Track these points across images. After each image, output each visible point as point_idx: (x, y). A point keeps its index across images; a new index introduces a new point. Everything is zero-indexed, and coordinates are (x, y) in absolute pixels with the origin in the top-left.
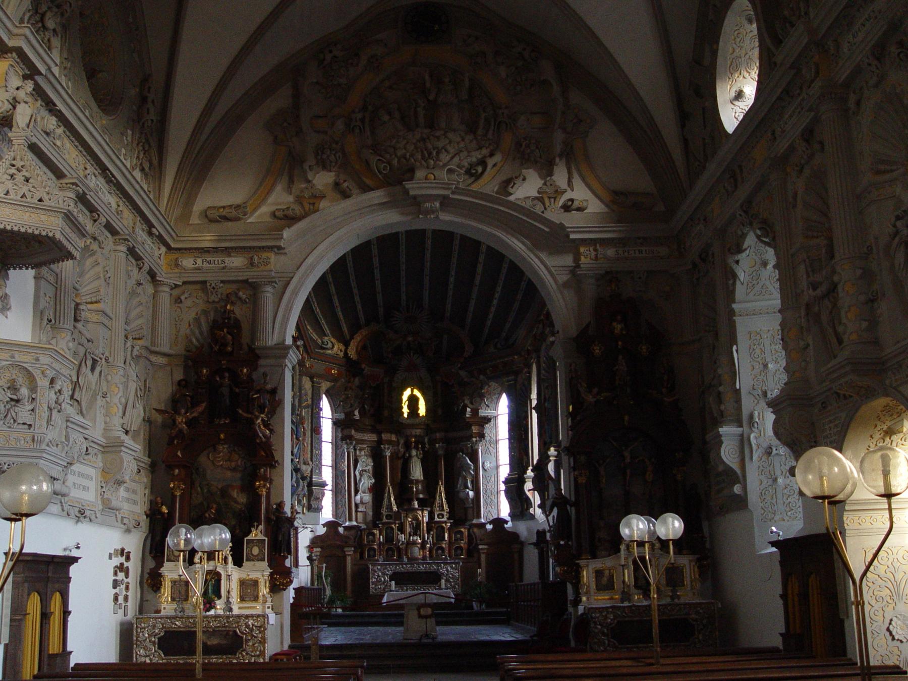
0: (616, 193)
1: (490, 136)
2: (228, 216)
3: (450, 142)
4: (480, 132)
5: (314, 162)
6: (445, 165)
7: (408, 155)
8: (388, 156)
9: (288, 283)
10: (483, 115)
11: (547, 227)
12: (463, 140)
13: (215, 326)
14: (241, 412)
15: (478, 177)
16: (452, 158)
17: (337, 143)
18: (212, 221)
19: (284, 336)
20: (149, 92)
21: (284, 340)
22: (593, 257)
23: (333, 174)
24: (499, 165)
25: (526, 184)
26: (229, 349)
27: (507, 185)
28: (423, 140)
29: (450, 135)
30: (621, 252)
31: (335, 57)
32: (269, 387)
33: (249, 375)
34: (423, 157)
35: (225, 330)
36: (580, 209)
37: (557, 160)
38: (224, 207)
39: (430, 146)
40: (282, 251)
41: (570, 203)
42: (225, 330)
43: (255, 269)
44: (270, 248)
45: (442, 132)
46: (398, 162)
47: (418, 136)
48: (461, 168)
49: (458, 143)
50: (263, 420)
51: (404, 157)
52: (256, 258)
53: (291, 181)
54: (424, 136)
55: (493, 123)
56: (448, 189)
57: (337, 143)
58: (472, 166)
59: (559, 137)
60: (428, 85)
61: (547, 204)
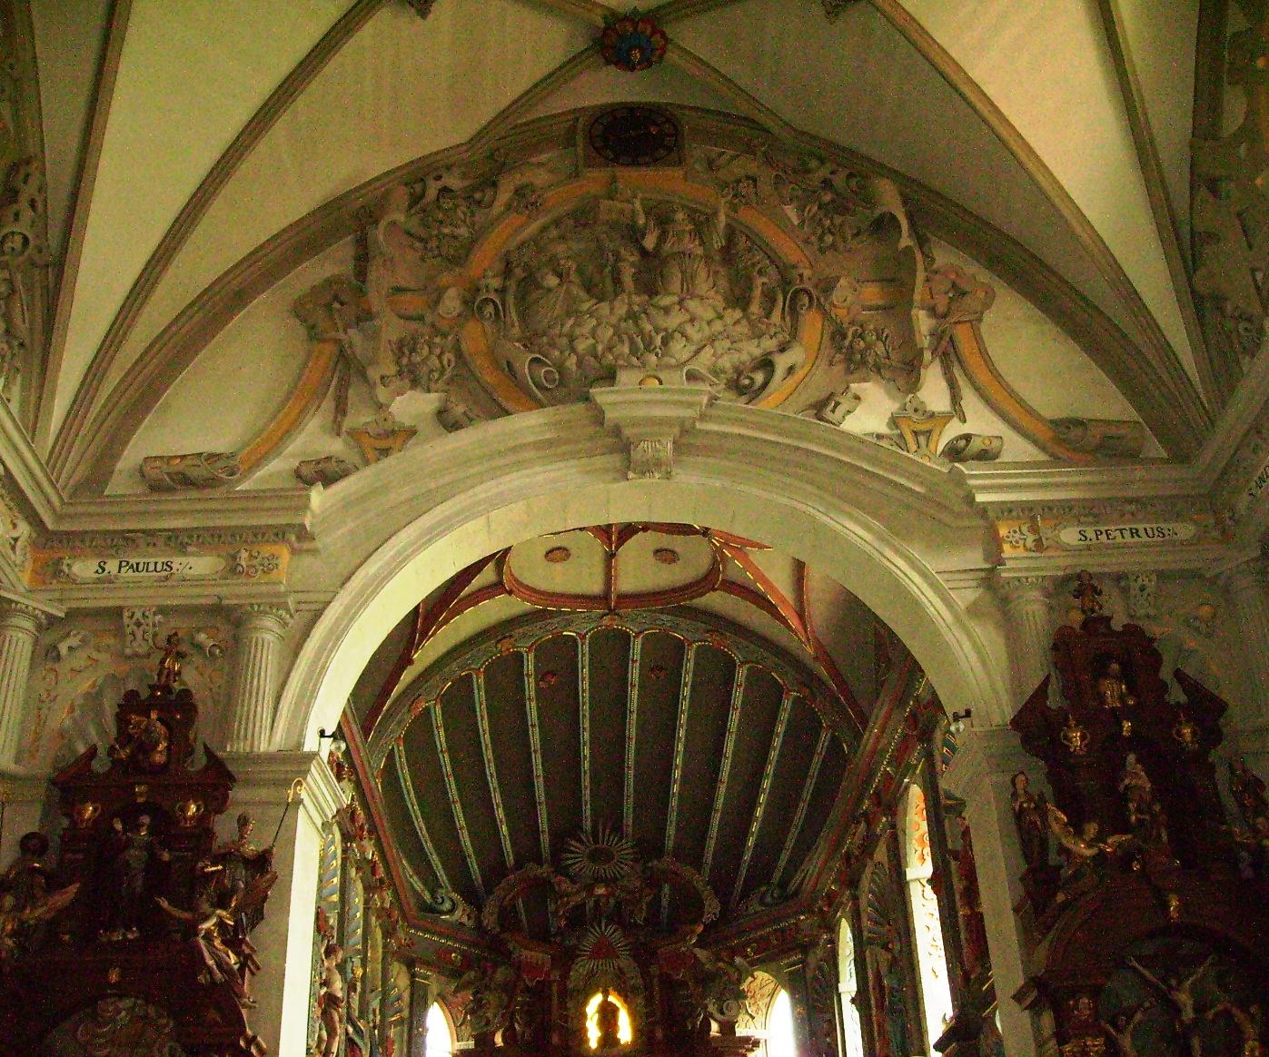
0: (1056, 423)
1: (776, 317)
2: (194, 473)
3: (692, 320)
4: (755, 308)
5: (393, 369)
6: (681, 365)
7: (600, 348)
9: (318, 615)
10: (759, 281)
11: (922, 483)
13: (131, 705)
14: (165, 904)
16: (697, 352)
17: (445, 336)
18: (156, 487)
19: (301, 735)
20: (25, 182)
21: (300, 745)
22: (1030, 543)
23: (433, 396)
24: (800, 374)
26: (159, 758)
28: (632, 316)
29: (692, 305)
30: (1090, 533)
31: (445, 190)
32: (251, 848)
33: (202, 819)
34: (634, 350)
35: (154, 716)
37: (927, 356)
38: (183, 457)
39: (648, 327)
40: (306, 545)
41: (962, 443)
42: (154, 716)
43: (243, 579)
44: (279, 534)
45: (676, 299)
46: (579, 364)
47: (621, 310)
49: (709, 323)
50: (221, 924)
52: (244, 555)
53: (341, 409)
54: (636, 308)
55: (780, 298)
56: (690, 405)
57: (445, 336)
59: (923, 323)
60: (641, 221)
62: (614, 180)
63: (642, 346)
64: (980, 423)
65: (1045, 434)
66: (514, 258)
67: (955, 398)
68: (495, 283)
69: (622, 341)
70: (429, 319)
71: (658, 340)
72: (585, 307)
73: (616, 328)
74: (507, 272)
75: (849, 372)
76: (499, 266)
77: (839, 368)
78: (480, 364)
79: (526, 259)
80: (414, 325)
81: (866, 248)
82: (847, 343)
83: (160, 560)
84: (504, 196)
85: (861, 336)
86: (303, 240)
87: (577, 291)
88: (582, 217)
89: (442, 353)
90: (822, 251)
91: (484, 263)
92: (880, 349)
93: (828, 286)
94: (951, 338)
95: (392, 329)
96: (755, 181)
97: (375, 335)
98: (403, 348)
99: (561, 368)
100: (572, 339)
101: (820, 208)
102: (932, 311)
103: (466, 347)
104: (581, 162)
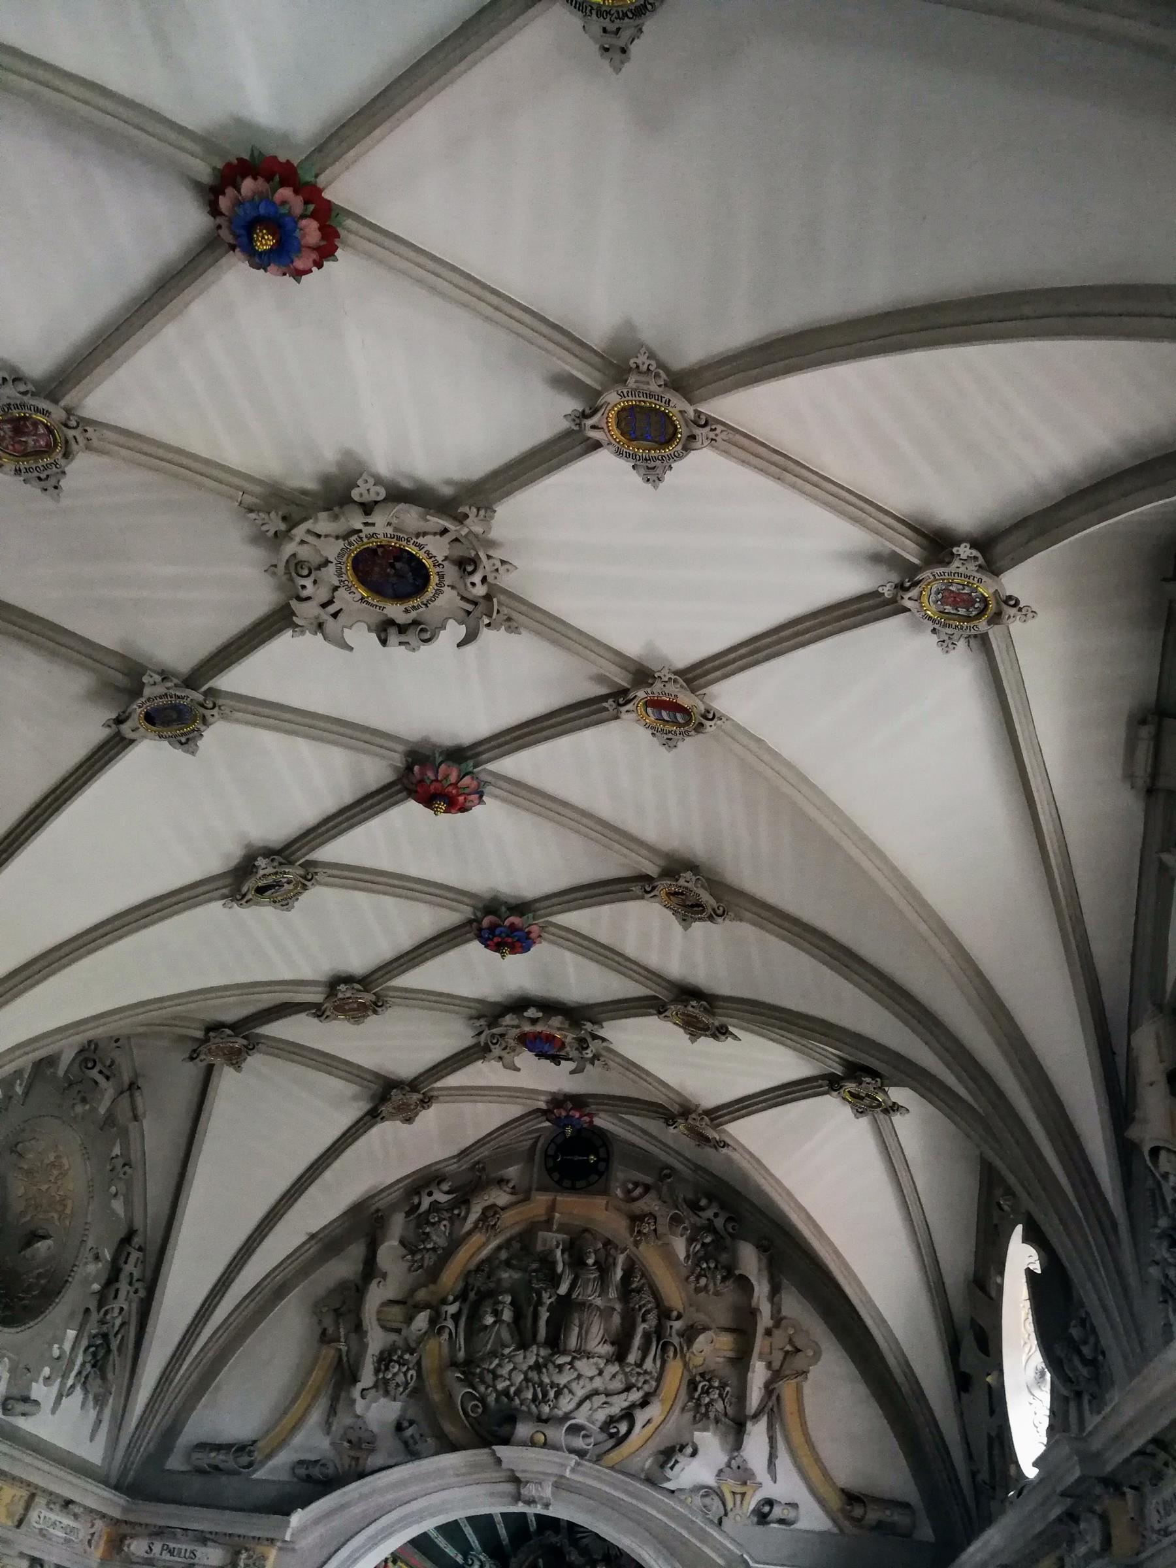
1: (648, 1365)
2: (221, 1466)
4: (632, 1358)
7: (512, 1390)
8: (482, 1389)
10: (641, 1328)
12: (601, 1373)
15: (621, 1440)
16: (580, 1404)
23: (398, 1405)
25: (695, 1463)
27: (668, 1455)
28: (537, 1367)
34: (535, 1398)
36: (782, 1521)
39: (546, 1380)
40: (290, 1546)
41: (766, 1509)
45: (568, 1359)
46: (497, 1400)
47: (531, 1362)
48: (593, 1423)
49: (591, 1378)
51: (506, 1393)
53: (332, 1411)
54: (541, 1360)
58: (612, 1420)
59: (758, 1374)
60: (560, 1269)
61: (730, 1505)
62: (552, 1208)
63: (540, 1396)
64: (786, 1486)
65: (835, 1502)
66: (471, 1280)
67: (772, 1457)
68: (452, 1309)
69: (527, 1388)
70: (404, 1332)
71: (552, 1394)
72: (507, 1351)
73: (526, 1374)
74: (462, 1296)
75: (695, 1420)
76: (460, 1285)
77: (689, 1416)
78: (432, 1381)
79: (478, 1284)
80: (394, 1337)
81: (729, 1292)
82: (696, 1395)
83: (189, 1548)
84: (474, 1216)
85: (708, 1393)
86: (327, 1244)
87: (506, 1335)
88: (525, 1238)
89: (408, 1369)
90: (698, 1290)
91: (450, 1277)
92: (719, 1406)
93: (690, 1334)
94: (778, 1398)
95: (376, 1340)
96: (655, 1218)
97: (364, 1347)
98: (385, 1360)
99: (483, 1400)
100: (496, 1377)
101: (703, 1245)
102: (769, 1365)
103: (424, 1363)
104: (535, 1186)
